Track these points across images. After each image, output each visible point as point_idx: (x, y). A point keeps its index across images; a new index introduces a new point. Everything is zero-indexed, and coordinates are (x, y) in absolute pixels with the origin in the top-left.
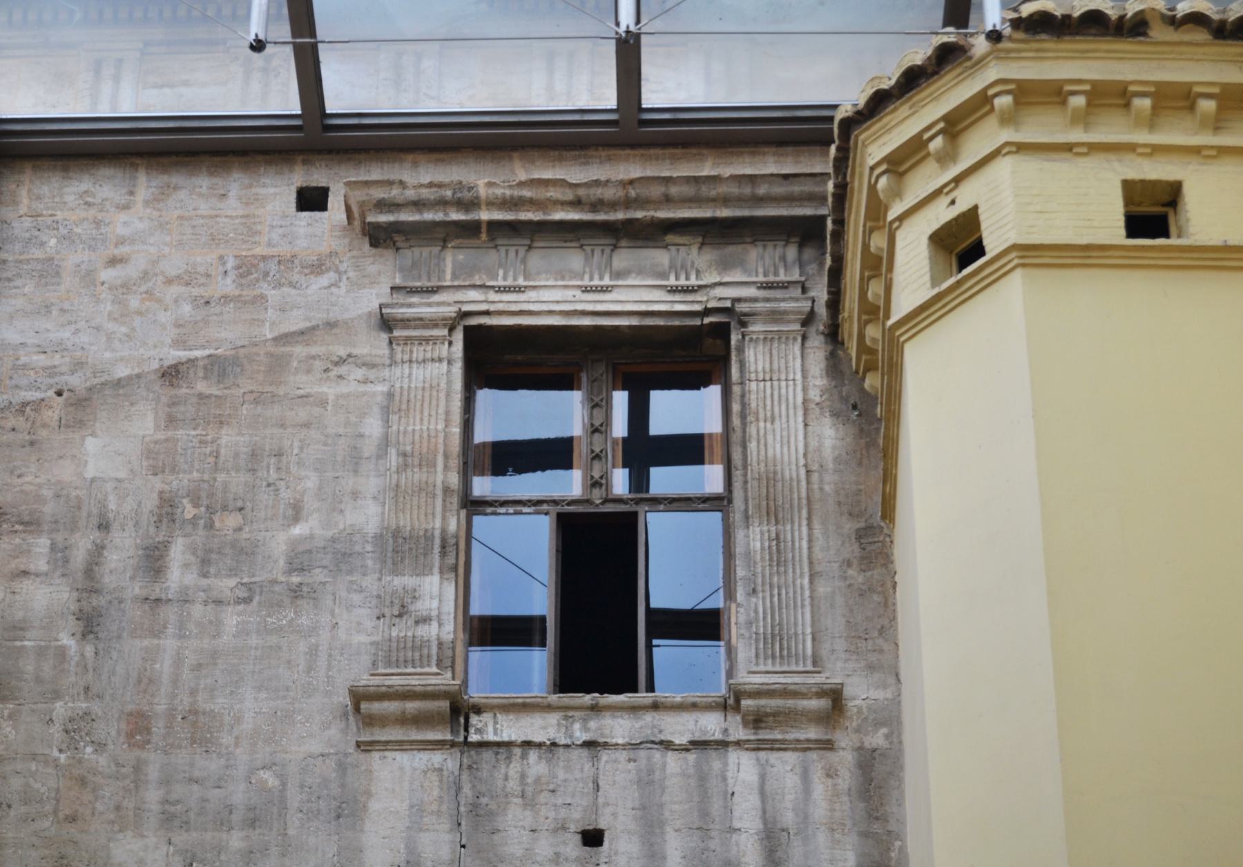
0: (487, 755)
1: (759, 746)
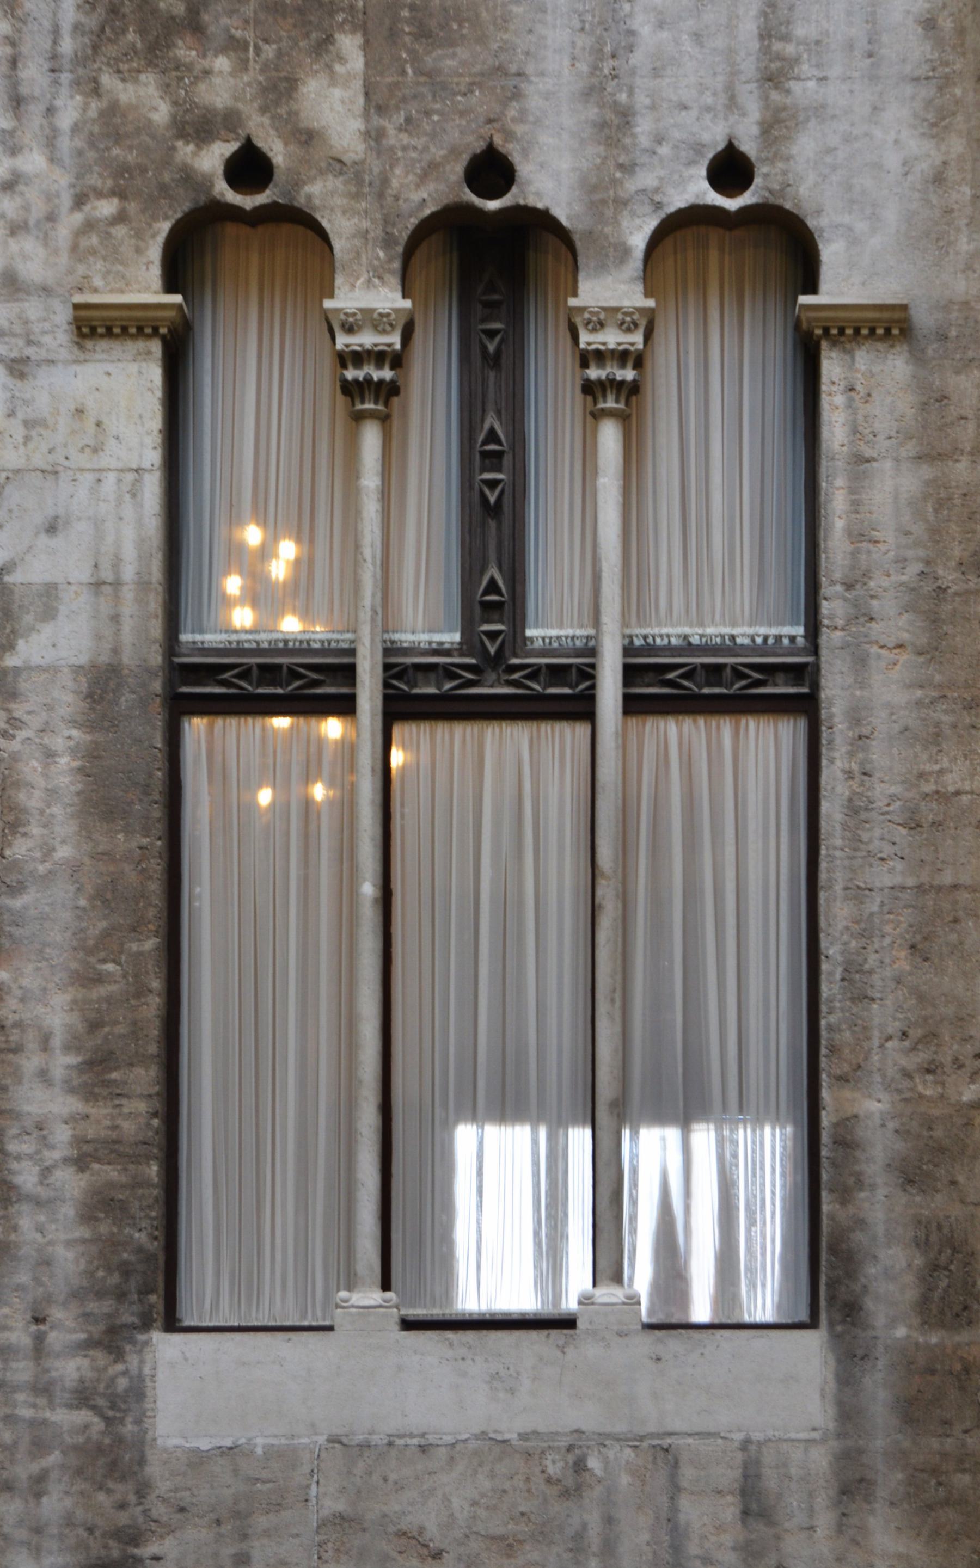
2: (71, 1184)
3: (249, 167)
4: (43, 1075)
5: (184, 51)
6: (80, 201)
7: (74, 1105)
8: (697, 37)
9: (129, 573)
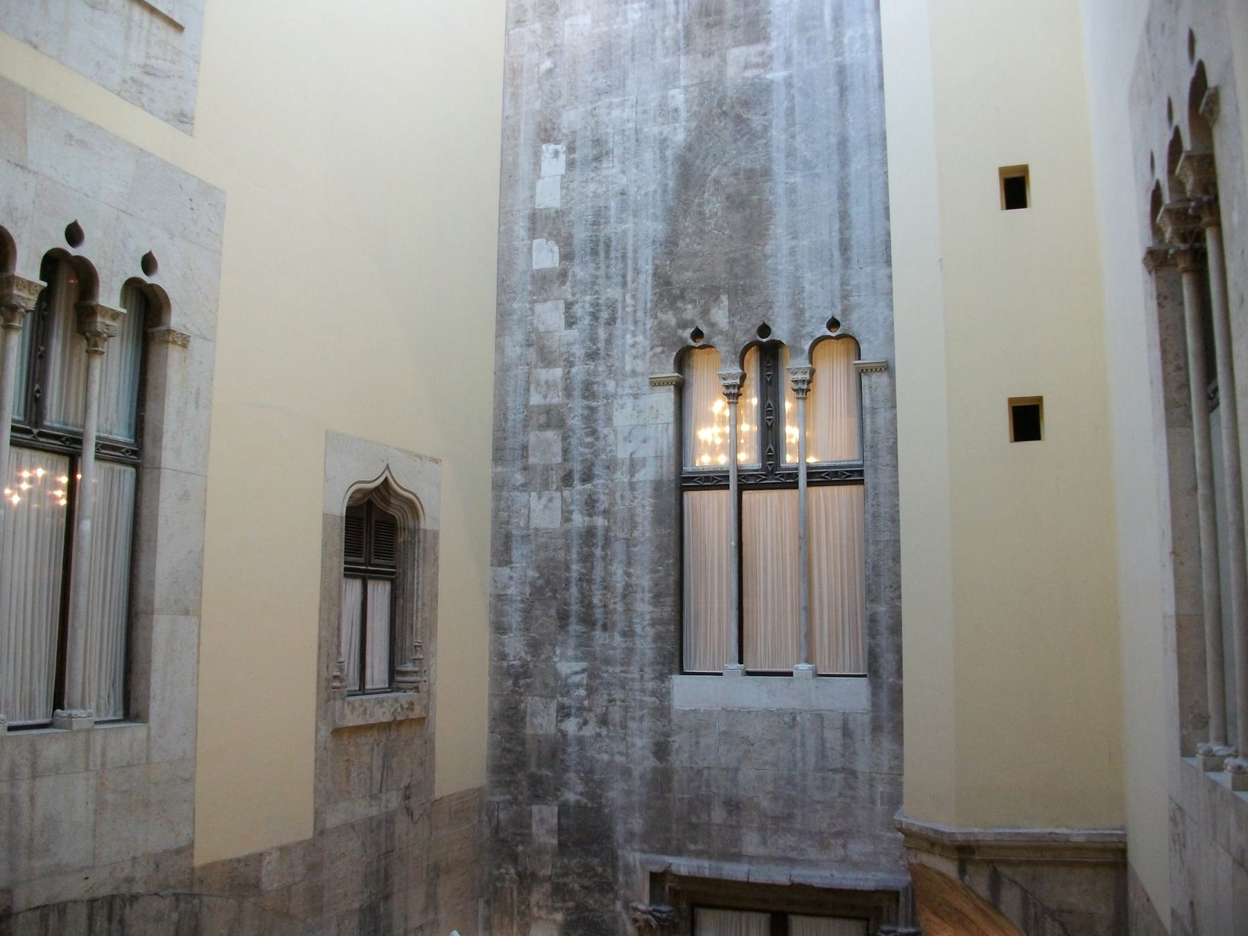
2: (650, 631)
3: (697, 334)
4: (642, 599)
5: (679, 304)
6: (652, 349)
7: (650, 608)
8: (822, 287)
9: (665, 453)
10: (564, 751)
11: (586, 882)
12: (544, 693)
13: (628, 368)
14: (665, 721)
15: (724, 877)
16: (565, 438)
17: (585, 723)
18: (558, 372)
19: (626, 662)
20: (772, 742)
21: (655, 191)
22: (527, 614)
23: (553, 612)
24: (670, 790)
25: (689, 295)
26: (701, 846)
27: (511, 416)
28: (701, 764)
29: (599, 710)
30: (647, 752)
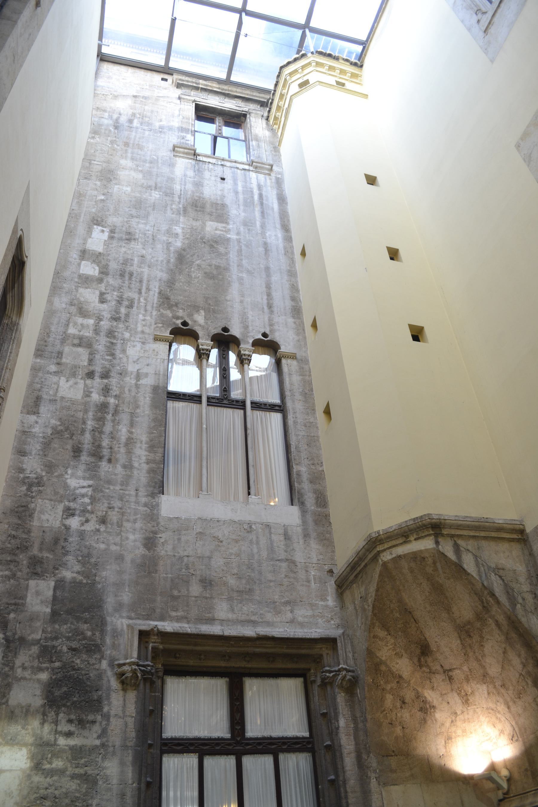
0: (201, 163)
1: (256, 172)
2: (145, 467)
4: (141, 448)
5: (174, 308)
6: (156, 324)
7: (147, 453)
9: (161, 373)
10: (66, 540)
11: (74, 645)
12: (53, 498)
13: (139, 329)
14: (154, 523)
15: (203, 633)
16: (91, 354)
17: (87, 521)
18: (91, 322)
19: (125, 483)
20: (237, 541)
21: (162, 261)
22: (47, 445)
23: (69, 447)
24: (156, 571)
25: (180, 306)
26: (180, 613)
27: (52, 336)
28: (182, 553)
29: (100, 514)
30: (138, 544)
